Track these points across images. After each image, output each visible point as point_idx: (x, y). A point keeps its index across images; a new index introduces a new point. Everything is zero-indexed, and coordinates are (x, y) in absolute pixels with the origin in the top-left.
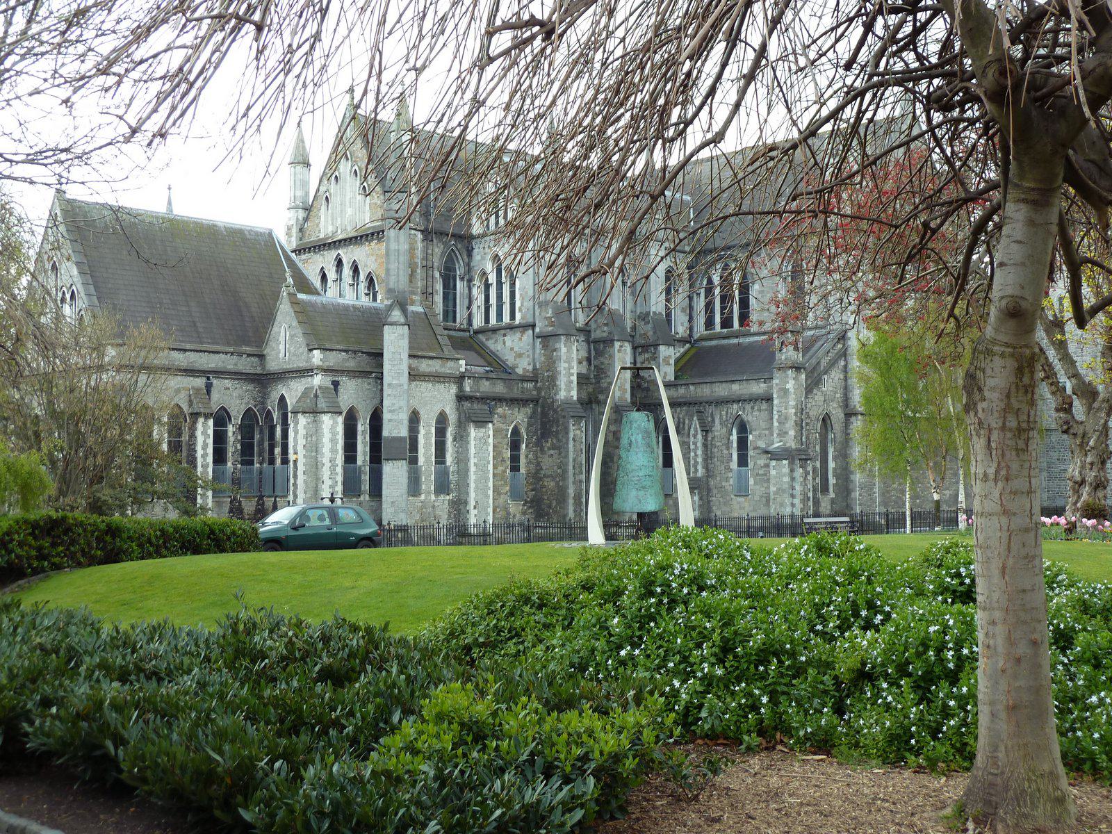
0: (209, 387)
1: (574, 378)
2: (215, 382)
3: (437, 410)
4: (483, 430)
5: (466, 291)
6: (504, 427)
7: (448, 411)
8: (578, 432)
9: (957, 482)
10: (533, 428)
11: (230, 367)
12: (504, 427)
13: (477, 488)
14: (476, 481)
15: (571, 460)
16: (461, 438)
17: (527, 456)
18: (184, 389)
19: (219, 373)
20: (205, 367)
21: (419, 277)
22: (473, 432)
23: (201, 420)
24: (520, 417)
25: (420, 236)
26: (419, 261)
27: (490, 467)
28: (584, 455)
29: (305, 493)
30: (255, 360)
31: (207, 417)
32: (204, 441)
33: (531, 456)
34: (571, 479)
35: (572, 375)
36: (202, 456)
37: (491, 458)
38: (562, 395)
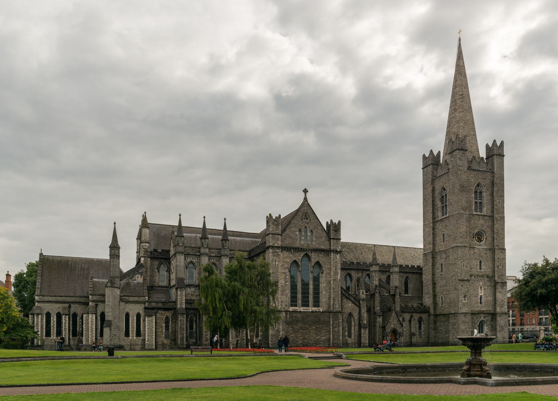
0: (70, 307)
1: (184, 301)
2: (72, 305)
3: (136, 312)
4: (151, 318)
5: (168, 275)
6: (162, 317)
7: (141, 312)
8: (182, 318)
9: (330, 334)
10: (174, 317)
11: (77, 301)
12: (162, 317)
13: (148, 336)
14: (148, 333)
15: (179, 327)
16: (144, 320)
17: (171, 326)
18: (61, 307)
19: (73, 303)
20: (69, 301)
21: (149, 272)
22: (147, 319)
23: (64, 316)
24: (169, 314)
25: (149, 259)
26: (149, 267)
27: (154, 329)
28: (185, 325)
29: (85, 336)
30: (86, 298)
31: (66, 315)
32: (65, 322)
33: (173, 326)
34: (179, 333)
35: (183, 300)
36: (64, 326)
37: (154, 326)
38: (178, 306)
